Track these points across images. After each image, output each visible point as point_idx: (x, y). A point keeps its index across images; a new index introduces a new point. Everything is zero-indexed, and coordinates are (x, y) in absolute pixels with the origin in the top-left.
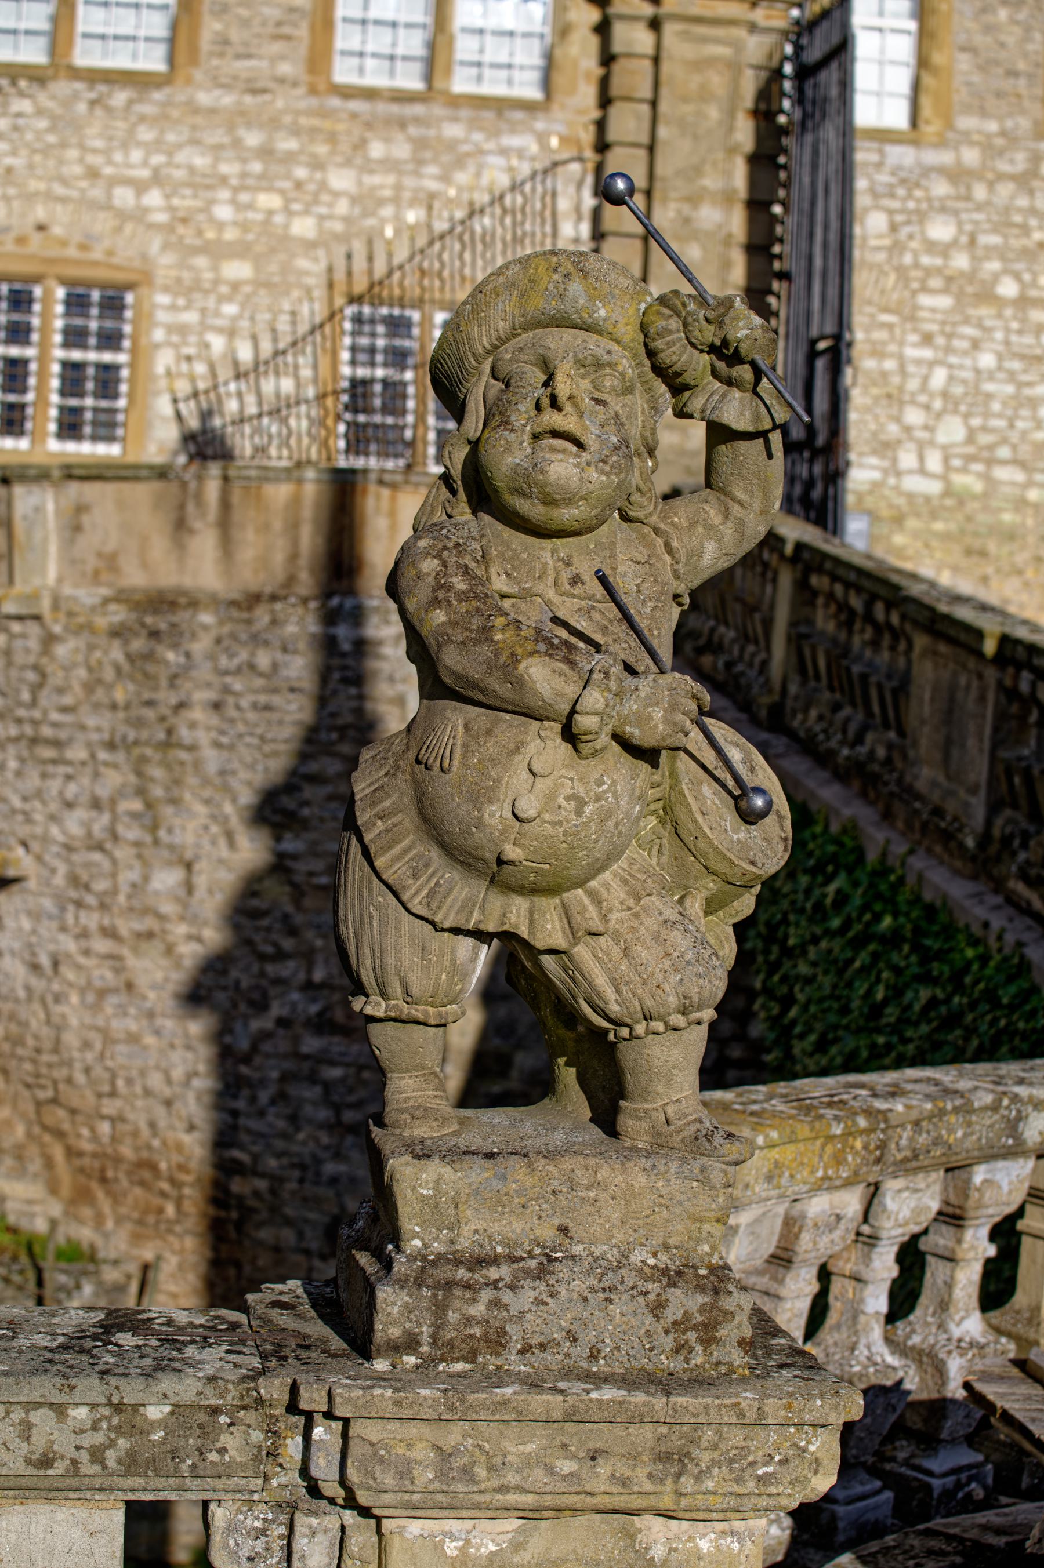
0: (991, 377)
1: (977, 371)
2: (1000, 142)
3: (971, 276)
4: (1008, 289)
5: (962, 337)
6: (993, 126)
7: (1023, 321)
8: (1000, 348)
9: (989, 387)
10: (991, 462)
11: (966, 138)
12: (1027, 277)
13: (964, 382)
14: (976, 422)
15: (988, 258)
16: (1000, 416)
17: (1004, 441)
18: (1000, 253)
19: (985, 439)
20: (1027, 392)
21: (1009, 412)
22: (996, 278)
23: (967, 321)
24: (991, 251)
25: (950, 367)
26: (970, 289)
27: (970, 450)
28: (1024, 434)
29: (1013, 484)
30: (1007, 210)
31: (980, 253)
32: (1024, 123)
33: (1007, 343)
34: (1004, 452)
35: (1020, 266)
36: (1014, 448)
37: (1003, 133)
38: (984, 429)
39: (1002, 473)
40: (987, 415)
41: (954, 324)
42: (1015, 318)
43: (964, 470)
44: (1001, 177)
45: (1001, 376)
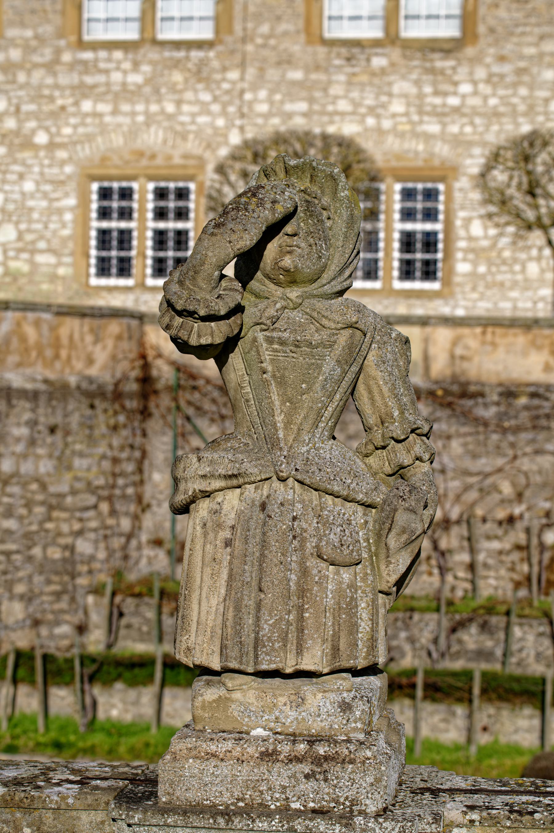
0: (32, 196)
1: (23, 194)
2: (34, 43)
3: (17, 133)
4: (41, 138)
5: (13, 172)
6: (29, 33)
7: (52, 158)
8: (37, 177)
9: (31, 203)
10: (33, 252)
11: (12, 43)
12: (53, 130)
13: (15, 201)
14: (23, 226)
15: (27, 119)
16: (38, 221)
17: (41, 238)
18: (35, 115)
19: (29, 237)
20: (56, 204)
21: (44, 219)
22: (33, 132)
23: (15, 162)
24: (30, 115)
25: (6, 192)
26: (17, 141)
27: (20, 245)
28: (55, 232)
29: (48, 265)
30: (40, 87)
31: (22, 116)
32: (47, 29)
33: (42, 174)
34: (42, 245)
35: (48, 123)
36: (48, 241)
37: (36, 37)
38: (29, 231)
39: (41, 259)
40: (30, 221)
41: (7, 164)
42: (46, 157)
43: (16, 258)
44: (36, 66)
45: (38, 195)
